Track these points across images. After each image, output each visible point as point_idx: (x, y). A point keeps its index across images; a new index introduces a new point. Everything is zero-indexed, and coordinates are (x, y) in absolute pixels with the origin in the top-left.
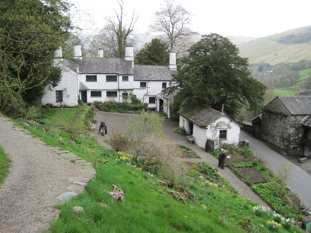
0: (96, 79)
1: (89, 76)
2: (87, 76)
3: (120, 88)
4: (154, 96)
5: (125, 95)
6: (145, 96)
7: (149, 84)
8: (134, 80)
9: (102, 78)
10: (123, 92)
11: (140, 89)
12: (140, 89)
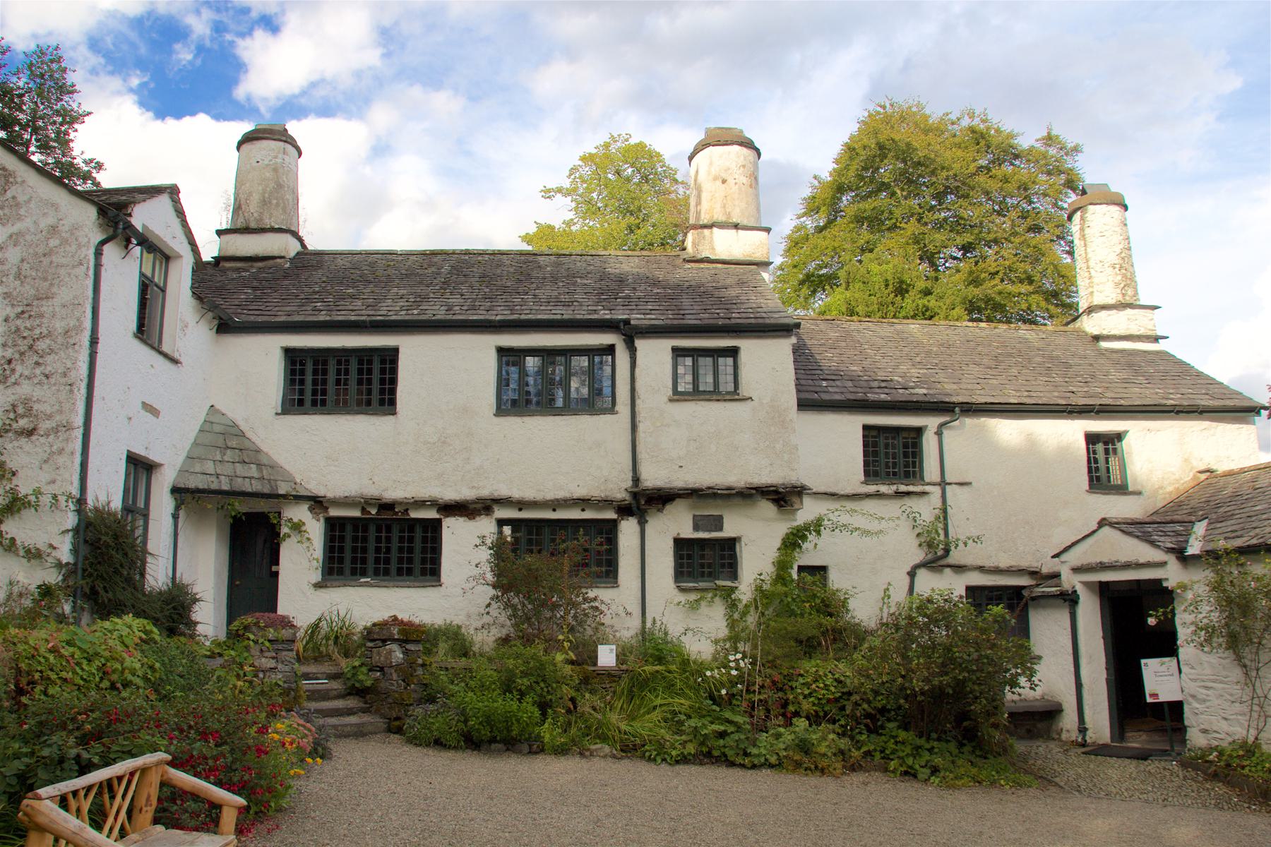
0: (393, 392)
1: (321, 356)
2: (289, 352)
3: (654, 477)
4: (1021, 572)
5: (705, 561)
6: (922, 574)
7: (954, 448)
8: (805, 405)
9: (447, 375)
10: (688, 532)
11: (868, 496)
12: (868, 496)
